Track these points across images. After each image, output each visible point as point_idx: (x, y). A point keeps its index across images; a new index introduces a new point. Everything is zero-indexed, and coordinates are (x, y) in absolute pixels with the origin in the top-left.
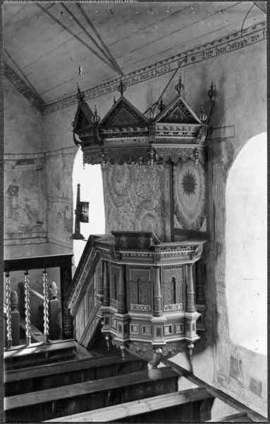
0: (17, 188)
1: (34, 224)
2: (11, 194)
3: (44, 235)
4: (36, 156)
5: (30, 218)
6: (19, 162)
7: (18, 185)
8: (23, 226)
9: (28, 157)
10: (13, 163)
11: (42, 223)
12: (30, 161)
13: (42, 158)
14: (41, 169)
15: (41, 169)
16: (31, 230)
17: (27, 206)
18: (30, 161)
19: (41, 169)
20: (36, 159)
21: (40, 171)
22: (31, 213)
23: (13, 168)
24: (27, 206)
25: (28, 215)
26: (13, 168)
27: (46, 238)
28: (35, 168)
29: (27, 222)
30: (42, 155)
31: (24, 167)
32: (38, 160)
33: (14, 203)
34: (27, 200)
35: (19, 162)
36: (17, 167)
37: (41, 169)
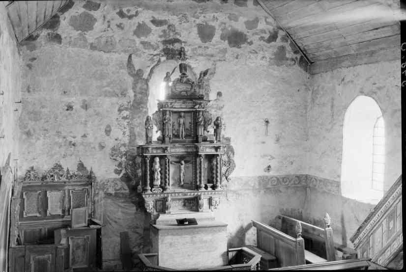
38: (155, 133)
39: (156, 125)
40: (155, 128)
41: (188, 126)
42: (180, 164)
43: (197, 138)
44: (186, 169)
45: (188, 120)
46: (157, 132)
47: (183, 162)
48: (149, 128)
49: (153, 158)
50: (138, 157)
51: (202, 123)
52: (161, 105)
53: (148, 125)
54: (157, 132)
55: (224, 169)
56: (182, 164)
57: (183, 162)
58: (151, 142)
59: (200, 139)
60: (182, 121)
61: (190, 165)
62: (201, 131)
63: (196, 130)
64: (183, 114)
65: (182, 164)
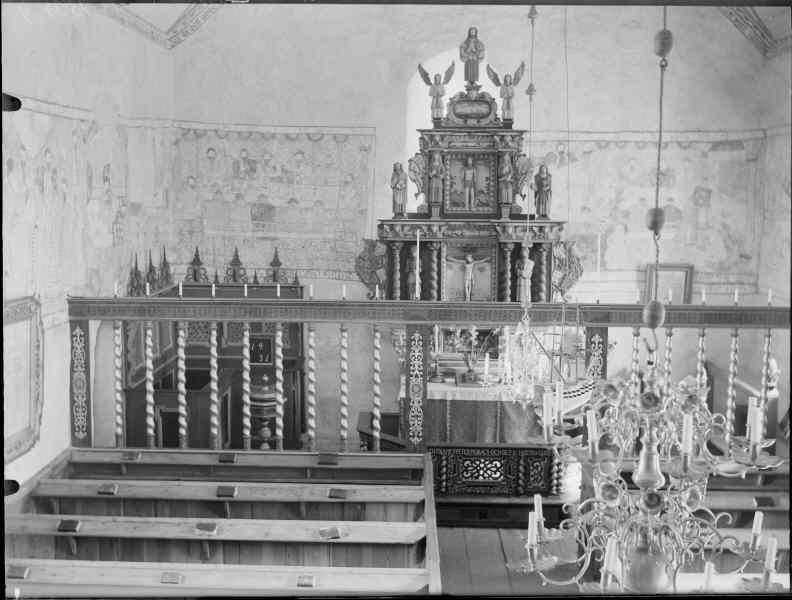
0: (709, 192)
1: (735, 257)
2: (696, 204)
3: (752, 280)
4: (748, 135)
5: (727, 247)
6: (716, 146)
7: (711, 187)
8: (714, 260)
9: (733, 137)
10: (706, 148)
11: (748, 257)
12: (737, 145)
13: (756, 139)
14: (755, 160)
15: (754, 159)
16: (729, 268)
17: (725, 226)
18: (737, 145)
19: (755, 160)
20: (746, 141)
21: (752, 164)
22: (731, 241)
23: (705, 155)
24: (725, 226)
25: (725, 241)
26: (705, 155)
27: (755, 285)
28: (744, 158)
29: (722, 254)
30: (760, 134)
31: (725, 155)
32: (751, 143)
33: (702, 220)
34: (724, 215)
35: (716, 146)
36: (710, 154)
37: (754, 159)
38: (414, 198)
39: (414, 181)
40: (412, 188)
41: (482, 185)
42: (464, 261)
43: (499, 206)
44: (477, 272)
45: (483, 175)
46: (416, 195)
47: (470, 259)
48: (398, 186)
49: (408, 245)
50: (379, 244)
51: (509, 179)
52: (427, 138)
53: (396, 180)
54: (416, 195)
55: (557, 276)
56: (468, 262)
57: (470, 259)
58: (401, 214)
59: (505, 211)
60: (469, 174)
61: (488, 267)
62: (507, 194)
63: (498, 192)
64: (470, 161)
65: (468, 262)
